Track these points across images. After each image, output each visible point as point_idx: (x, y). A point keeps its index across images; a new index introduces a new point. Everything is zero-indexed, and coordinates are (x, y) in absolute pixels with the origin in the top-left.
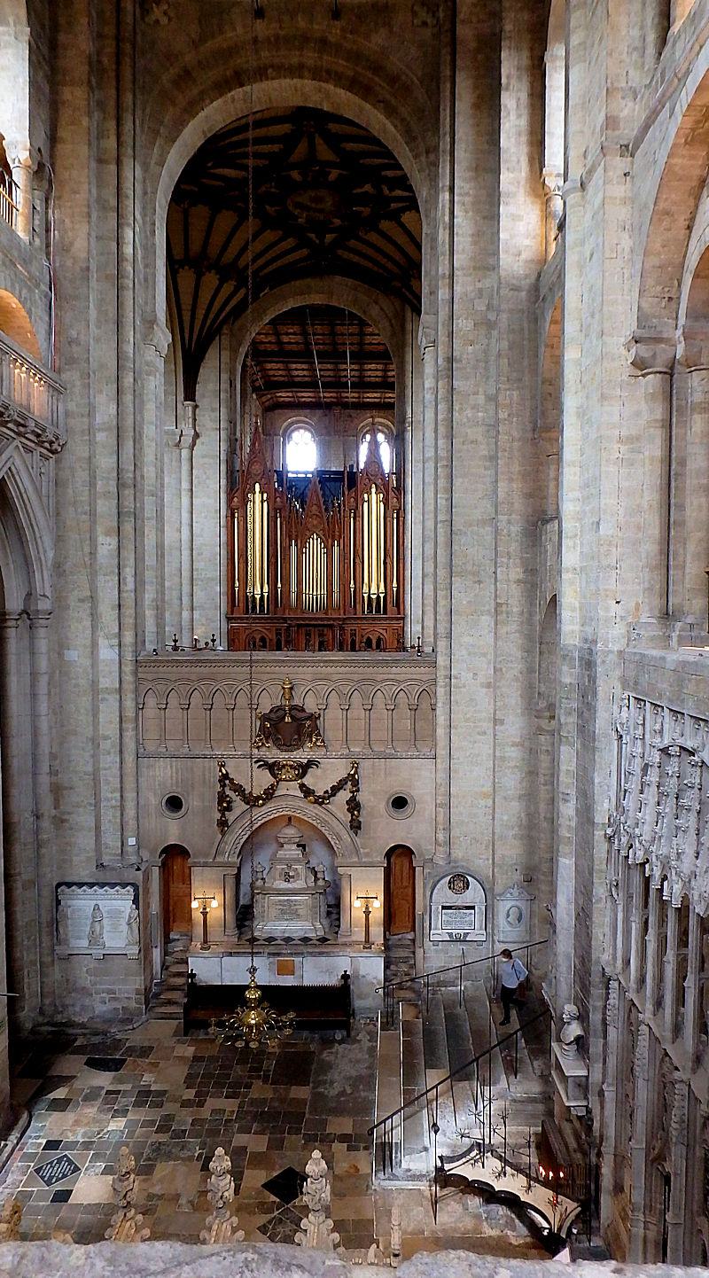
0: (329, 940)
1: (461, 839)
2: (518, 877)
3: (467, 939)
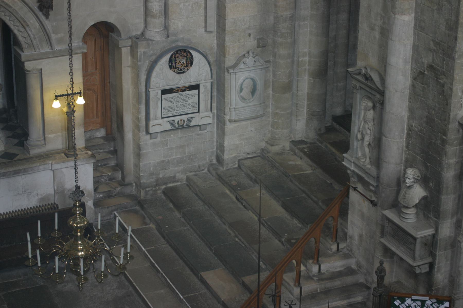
0: (16, 155)
1: (181, 6)
2: (251, 43)
3: (193, 124)
